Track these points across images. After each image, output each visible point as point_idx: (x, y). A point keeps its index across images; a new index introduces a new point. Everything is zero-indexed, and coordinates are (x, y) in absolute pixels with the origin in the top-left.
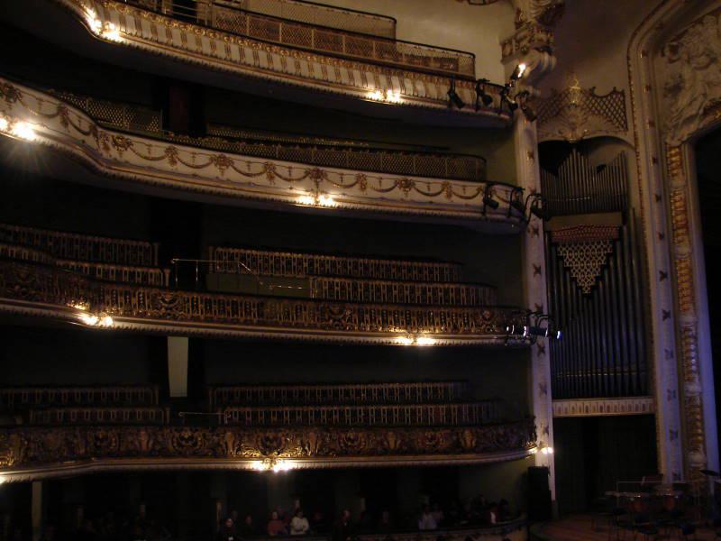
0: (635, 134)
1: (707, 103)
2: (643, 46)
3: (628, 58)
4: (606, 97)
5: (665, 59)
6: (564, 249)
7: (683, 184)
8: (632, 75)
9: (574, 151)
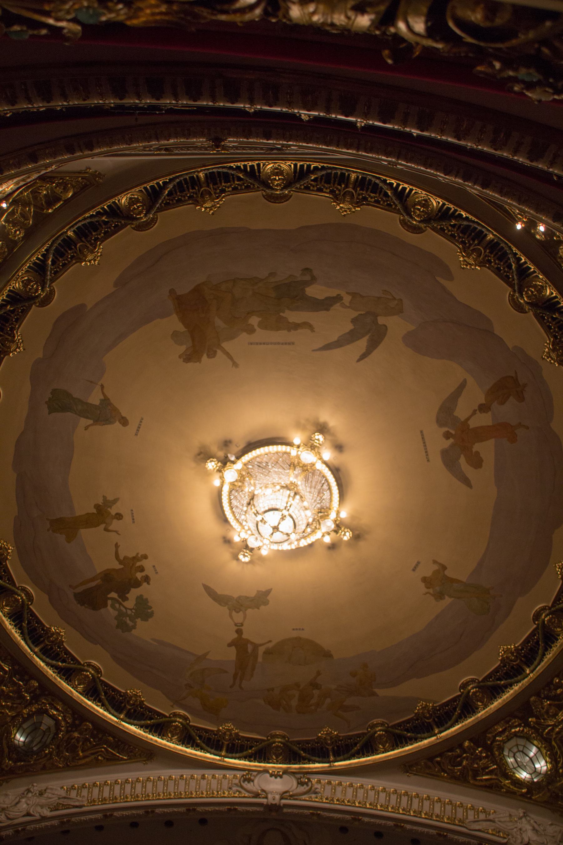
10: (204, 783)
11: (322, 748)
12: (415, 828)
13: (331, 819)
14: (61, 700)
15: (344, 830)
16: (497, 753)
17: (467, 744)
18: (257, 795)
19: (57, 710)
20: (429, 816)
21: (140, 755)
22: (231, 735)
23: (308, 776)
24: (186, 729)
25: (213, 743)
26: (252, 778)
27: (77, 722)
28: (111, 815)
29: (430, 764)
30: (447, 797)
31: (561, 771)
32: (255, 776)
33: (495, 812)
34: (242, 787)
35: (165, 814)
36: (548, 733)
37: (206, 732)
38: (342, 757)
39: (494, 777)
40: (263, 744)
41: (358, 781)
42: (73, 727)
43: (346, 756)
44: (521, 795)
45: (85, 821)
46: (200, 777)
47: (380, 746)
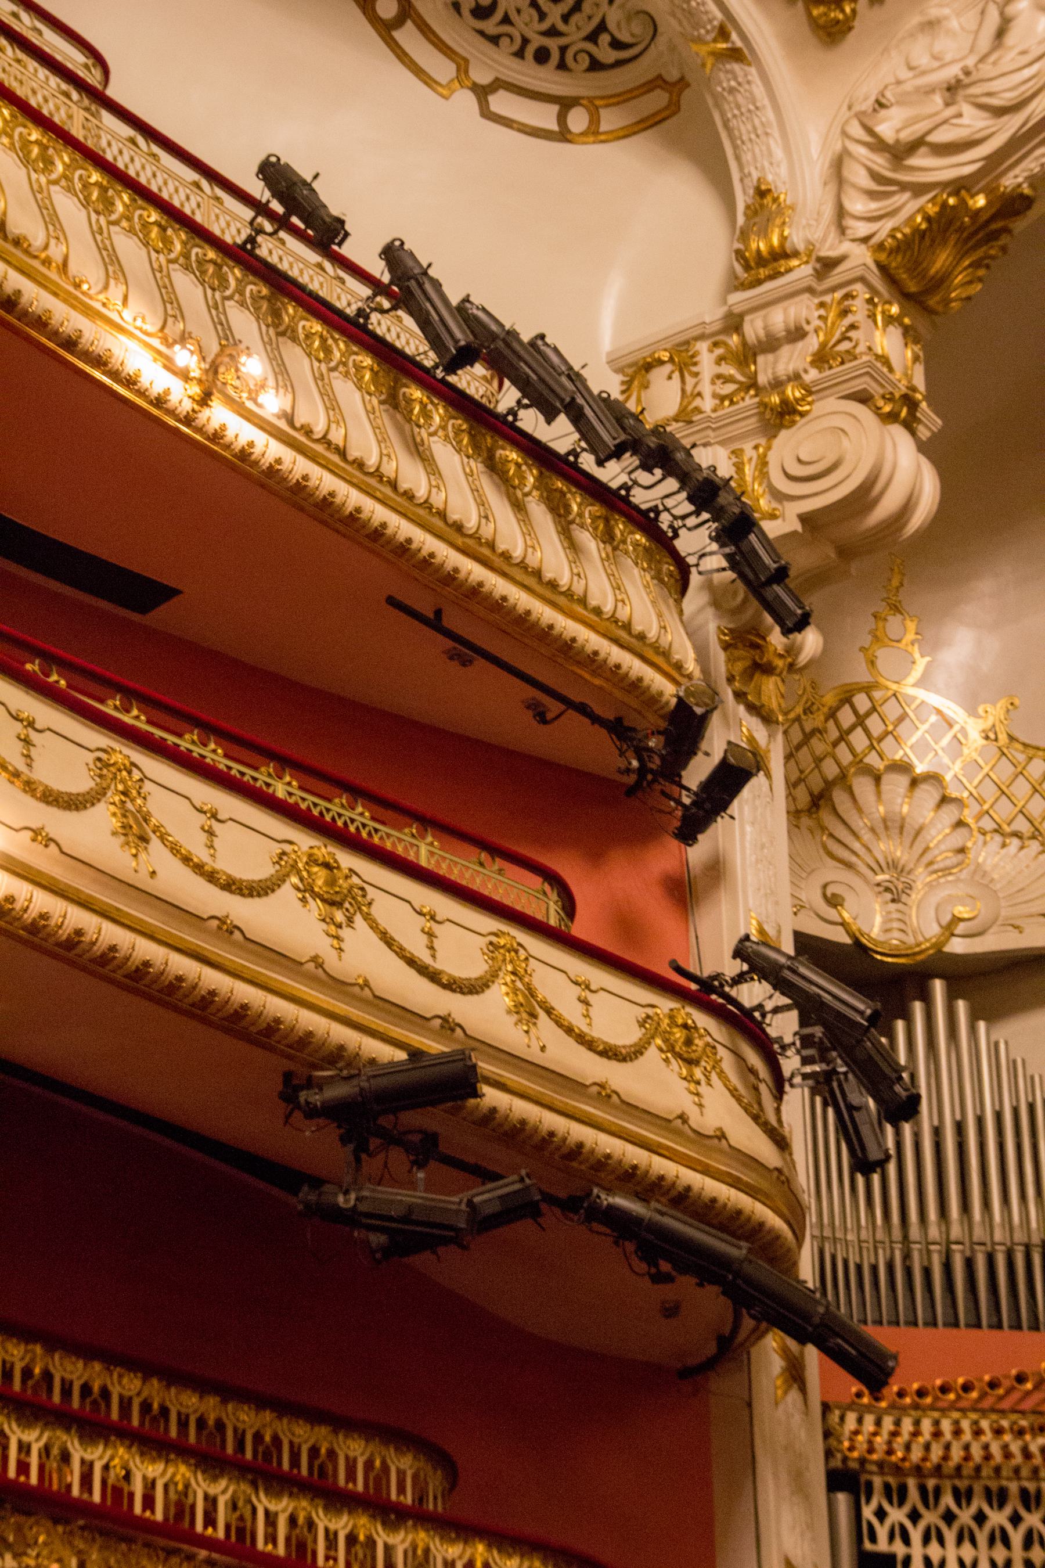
6: (897, 1515)
9: (938, 986)
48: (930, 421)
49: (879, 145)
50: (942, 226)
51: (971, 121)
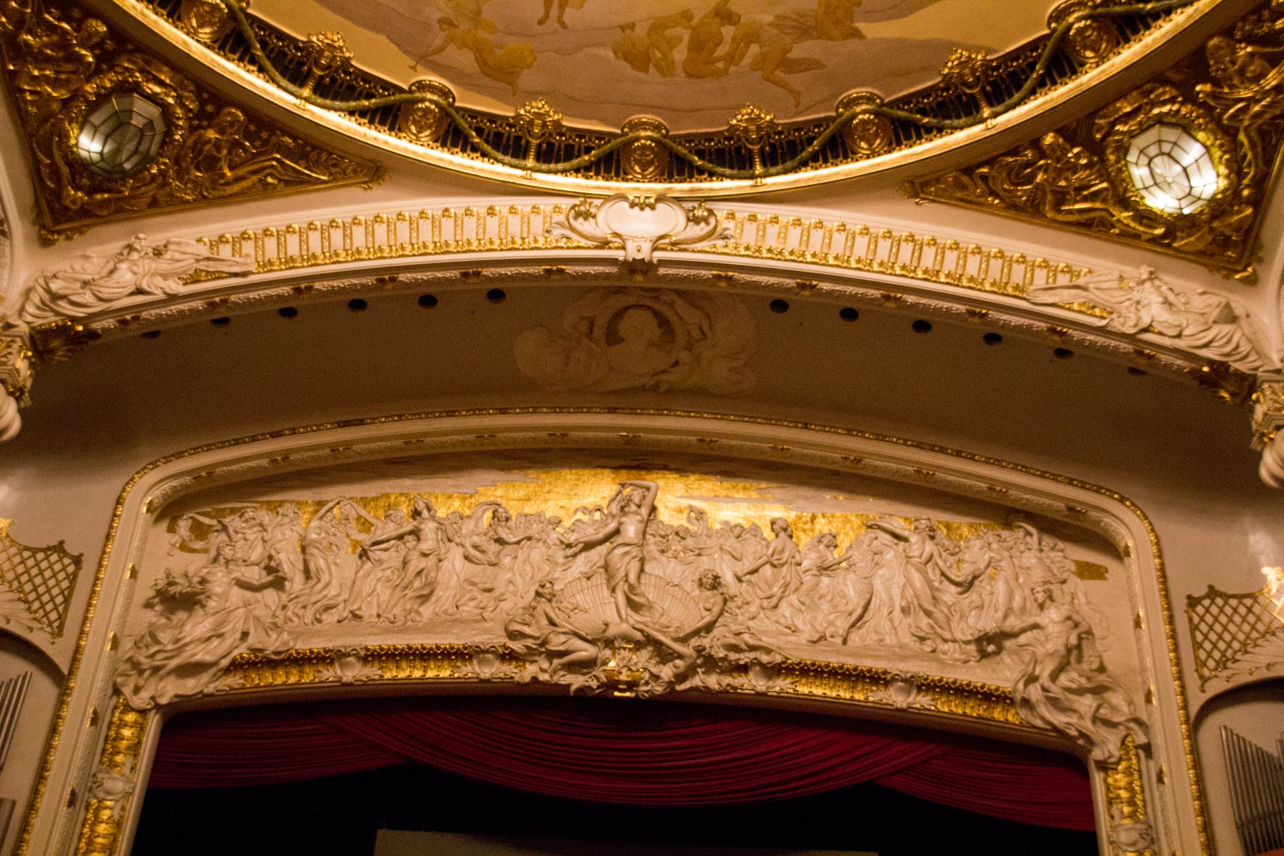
0: (78, 650)
1: (242, 651)
2: (155, 495)
3: (119, 501)
4: (35, 551)
5: (175, 539)
7: (125, 787)
8: (118, 534)
10: (492, 222)
11: (738, 149)
12: (923, 301)
13: (756, 285)
14: (167, 62)
15: (780, 306)
16: (1112, 158)
17: (1049, 139)
18: (604, 244)
19: (161, 83)
20: (956, 280)
21: (355, 171)
22: (544, 125)
23: (710, 205)
24: (448, 114)
25: (507, 141)
26: (593, 210)
27: (210, 108)
28: (309, 288)
29: (965, 179)
30: (992, 242)
31: (1246, 193)
32: (599, 208)
33: (1090, 272)
34: (572, 229)
35: (417, 283)
36: (1233, 116)
37: (491, 122)
38: (780, 167)
39: (1098, 205)
40: (614, 142)
41: (810, 214)
42: (201, 118)
43: (789, 164)
44: (1148, 241)
45: (259, 302)
46: (483, 211)
47: (863, 145)
48: (27, 401)
49: (48, 291)
50: (63, 331)
51: (88, 298)
